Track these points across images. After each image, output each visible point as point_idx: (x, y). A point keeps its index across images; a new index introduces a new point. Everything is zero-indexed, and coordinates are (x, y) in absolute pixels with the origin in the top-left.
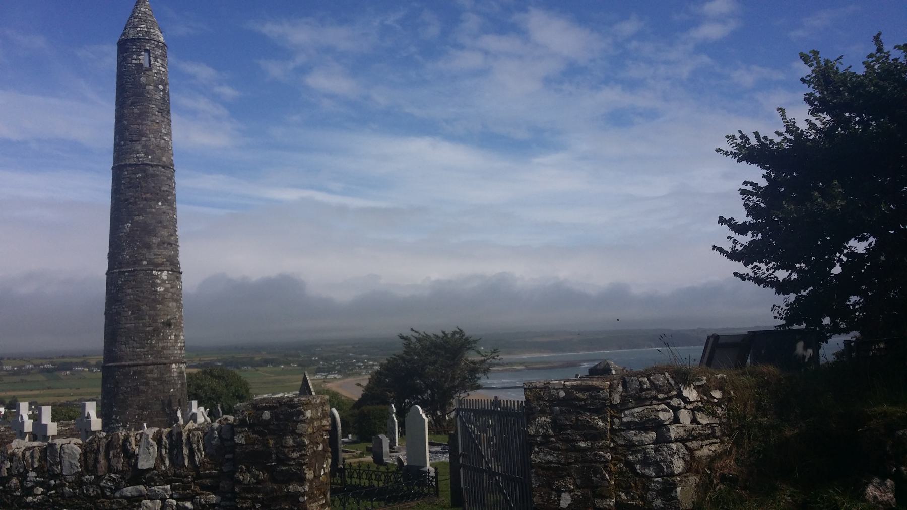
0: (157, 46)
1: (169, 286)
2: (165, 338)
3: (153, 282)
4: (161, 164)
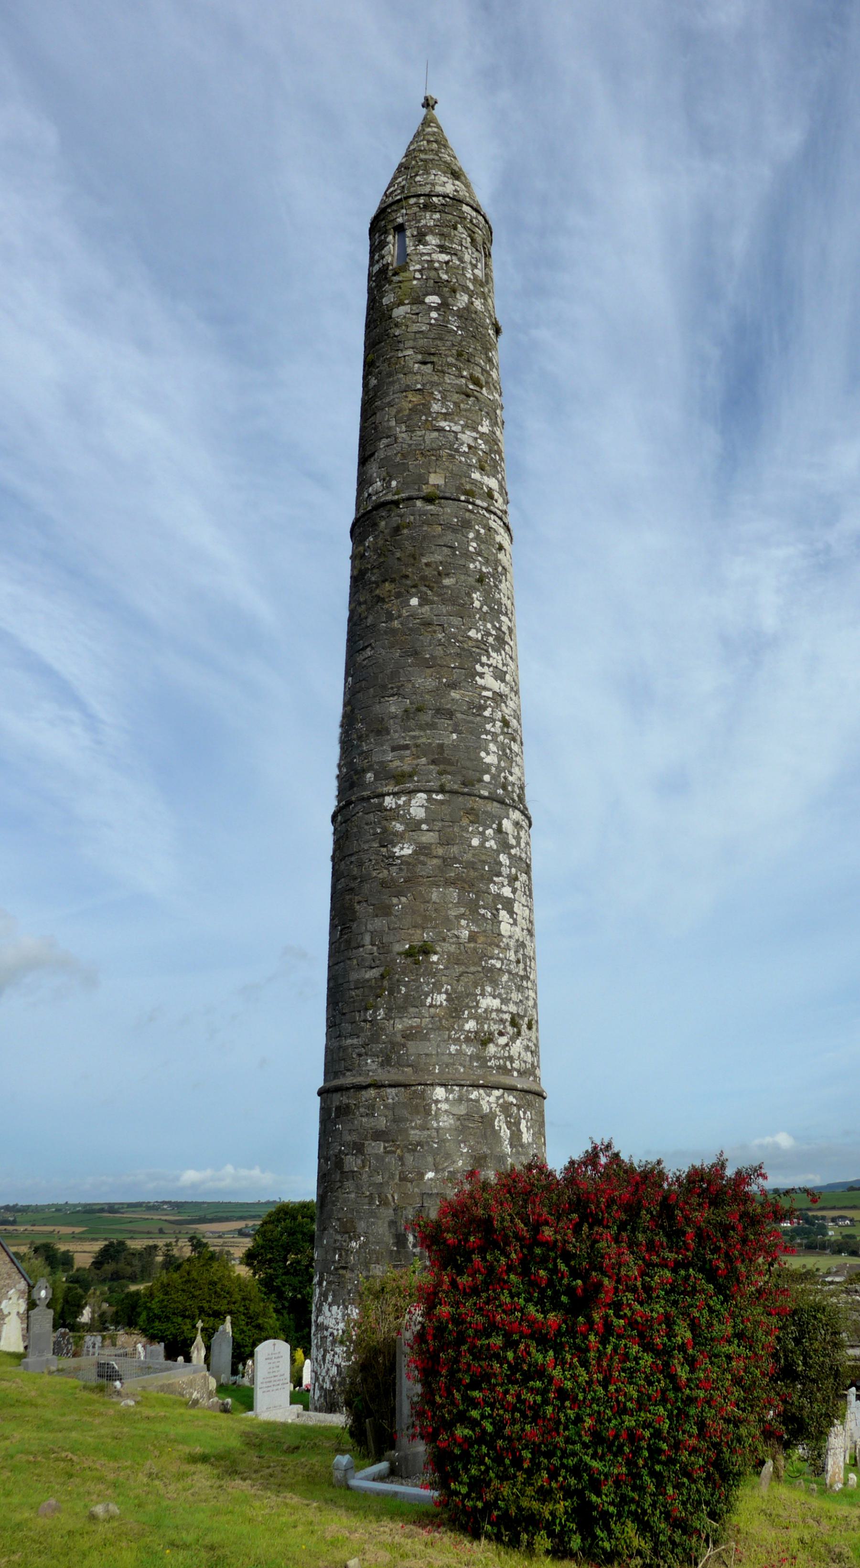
0: (426, 207)
1: (428, 838)
2: (414, 1001)
3: (385, 830)
4: (426, 490)
